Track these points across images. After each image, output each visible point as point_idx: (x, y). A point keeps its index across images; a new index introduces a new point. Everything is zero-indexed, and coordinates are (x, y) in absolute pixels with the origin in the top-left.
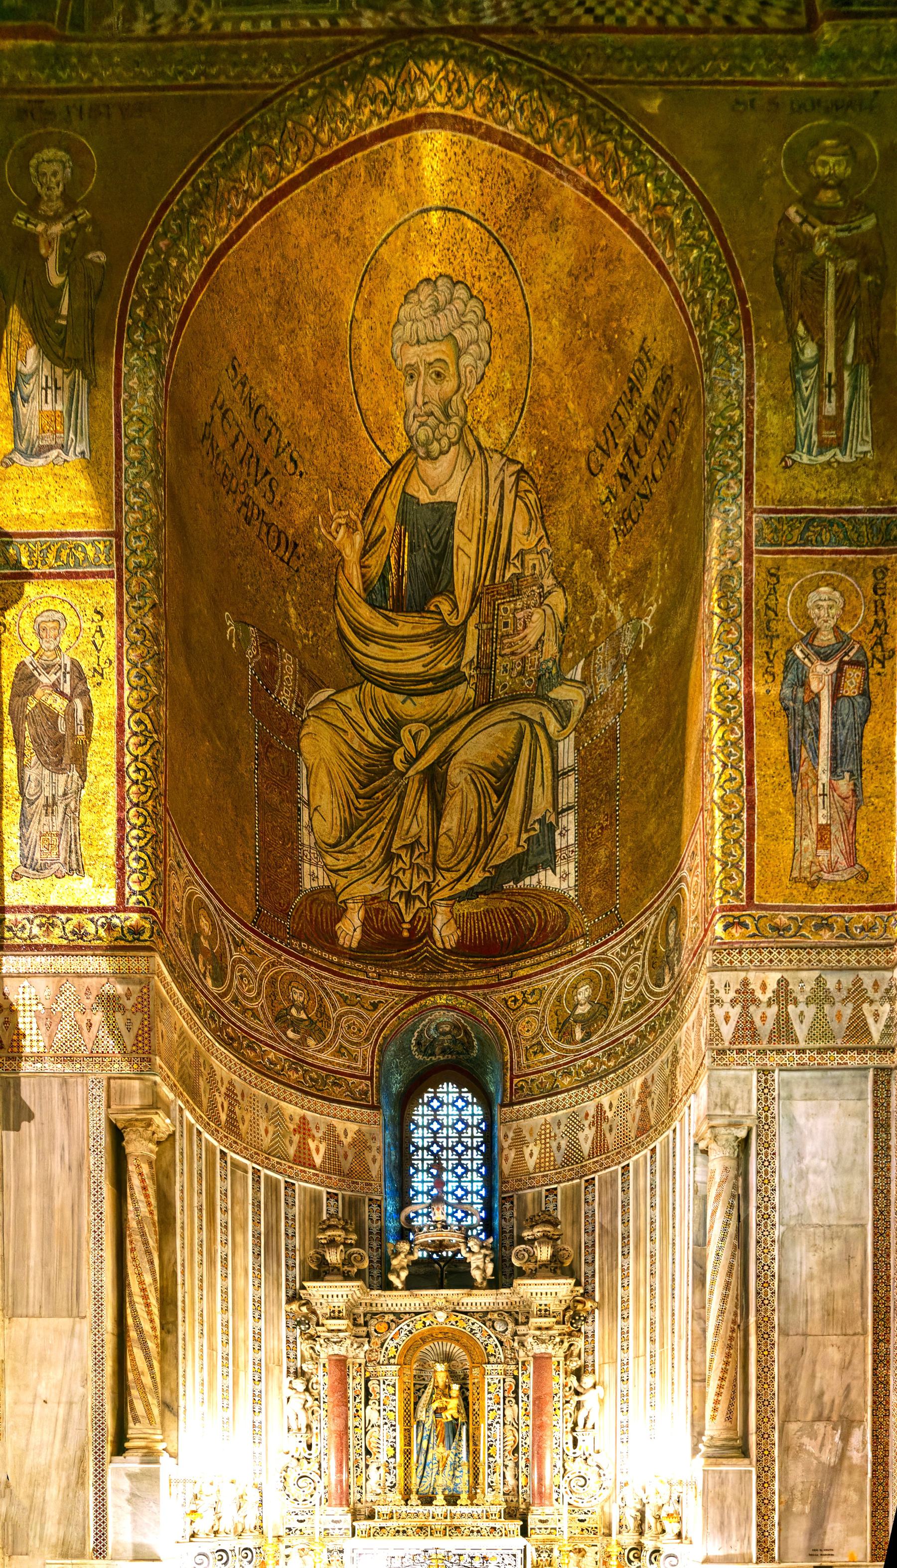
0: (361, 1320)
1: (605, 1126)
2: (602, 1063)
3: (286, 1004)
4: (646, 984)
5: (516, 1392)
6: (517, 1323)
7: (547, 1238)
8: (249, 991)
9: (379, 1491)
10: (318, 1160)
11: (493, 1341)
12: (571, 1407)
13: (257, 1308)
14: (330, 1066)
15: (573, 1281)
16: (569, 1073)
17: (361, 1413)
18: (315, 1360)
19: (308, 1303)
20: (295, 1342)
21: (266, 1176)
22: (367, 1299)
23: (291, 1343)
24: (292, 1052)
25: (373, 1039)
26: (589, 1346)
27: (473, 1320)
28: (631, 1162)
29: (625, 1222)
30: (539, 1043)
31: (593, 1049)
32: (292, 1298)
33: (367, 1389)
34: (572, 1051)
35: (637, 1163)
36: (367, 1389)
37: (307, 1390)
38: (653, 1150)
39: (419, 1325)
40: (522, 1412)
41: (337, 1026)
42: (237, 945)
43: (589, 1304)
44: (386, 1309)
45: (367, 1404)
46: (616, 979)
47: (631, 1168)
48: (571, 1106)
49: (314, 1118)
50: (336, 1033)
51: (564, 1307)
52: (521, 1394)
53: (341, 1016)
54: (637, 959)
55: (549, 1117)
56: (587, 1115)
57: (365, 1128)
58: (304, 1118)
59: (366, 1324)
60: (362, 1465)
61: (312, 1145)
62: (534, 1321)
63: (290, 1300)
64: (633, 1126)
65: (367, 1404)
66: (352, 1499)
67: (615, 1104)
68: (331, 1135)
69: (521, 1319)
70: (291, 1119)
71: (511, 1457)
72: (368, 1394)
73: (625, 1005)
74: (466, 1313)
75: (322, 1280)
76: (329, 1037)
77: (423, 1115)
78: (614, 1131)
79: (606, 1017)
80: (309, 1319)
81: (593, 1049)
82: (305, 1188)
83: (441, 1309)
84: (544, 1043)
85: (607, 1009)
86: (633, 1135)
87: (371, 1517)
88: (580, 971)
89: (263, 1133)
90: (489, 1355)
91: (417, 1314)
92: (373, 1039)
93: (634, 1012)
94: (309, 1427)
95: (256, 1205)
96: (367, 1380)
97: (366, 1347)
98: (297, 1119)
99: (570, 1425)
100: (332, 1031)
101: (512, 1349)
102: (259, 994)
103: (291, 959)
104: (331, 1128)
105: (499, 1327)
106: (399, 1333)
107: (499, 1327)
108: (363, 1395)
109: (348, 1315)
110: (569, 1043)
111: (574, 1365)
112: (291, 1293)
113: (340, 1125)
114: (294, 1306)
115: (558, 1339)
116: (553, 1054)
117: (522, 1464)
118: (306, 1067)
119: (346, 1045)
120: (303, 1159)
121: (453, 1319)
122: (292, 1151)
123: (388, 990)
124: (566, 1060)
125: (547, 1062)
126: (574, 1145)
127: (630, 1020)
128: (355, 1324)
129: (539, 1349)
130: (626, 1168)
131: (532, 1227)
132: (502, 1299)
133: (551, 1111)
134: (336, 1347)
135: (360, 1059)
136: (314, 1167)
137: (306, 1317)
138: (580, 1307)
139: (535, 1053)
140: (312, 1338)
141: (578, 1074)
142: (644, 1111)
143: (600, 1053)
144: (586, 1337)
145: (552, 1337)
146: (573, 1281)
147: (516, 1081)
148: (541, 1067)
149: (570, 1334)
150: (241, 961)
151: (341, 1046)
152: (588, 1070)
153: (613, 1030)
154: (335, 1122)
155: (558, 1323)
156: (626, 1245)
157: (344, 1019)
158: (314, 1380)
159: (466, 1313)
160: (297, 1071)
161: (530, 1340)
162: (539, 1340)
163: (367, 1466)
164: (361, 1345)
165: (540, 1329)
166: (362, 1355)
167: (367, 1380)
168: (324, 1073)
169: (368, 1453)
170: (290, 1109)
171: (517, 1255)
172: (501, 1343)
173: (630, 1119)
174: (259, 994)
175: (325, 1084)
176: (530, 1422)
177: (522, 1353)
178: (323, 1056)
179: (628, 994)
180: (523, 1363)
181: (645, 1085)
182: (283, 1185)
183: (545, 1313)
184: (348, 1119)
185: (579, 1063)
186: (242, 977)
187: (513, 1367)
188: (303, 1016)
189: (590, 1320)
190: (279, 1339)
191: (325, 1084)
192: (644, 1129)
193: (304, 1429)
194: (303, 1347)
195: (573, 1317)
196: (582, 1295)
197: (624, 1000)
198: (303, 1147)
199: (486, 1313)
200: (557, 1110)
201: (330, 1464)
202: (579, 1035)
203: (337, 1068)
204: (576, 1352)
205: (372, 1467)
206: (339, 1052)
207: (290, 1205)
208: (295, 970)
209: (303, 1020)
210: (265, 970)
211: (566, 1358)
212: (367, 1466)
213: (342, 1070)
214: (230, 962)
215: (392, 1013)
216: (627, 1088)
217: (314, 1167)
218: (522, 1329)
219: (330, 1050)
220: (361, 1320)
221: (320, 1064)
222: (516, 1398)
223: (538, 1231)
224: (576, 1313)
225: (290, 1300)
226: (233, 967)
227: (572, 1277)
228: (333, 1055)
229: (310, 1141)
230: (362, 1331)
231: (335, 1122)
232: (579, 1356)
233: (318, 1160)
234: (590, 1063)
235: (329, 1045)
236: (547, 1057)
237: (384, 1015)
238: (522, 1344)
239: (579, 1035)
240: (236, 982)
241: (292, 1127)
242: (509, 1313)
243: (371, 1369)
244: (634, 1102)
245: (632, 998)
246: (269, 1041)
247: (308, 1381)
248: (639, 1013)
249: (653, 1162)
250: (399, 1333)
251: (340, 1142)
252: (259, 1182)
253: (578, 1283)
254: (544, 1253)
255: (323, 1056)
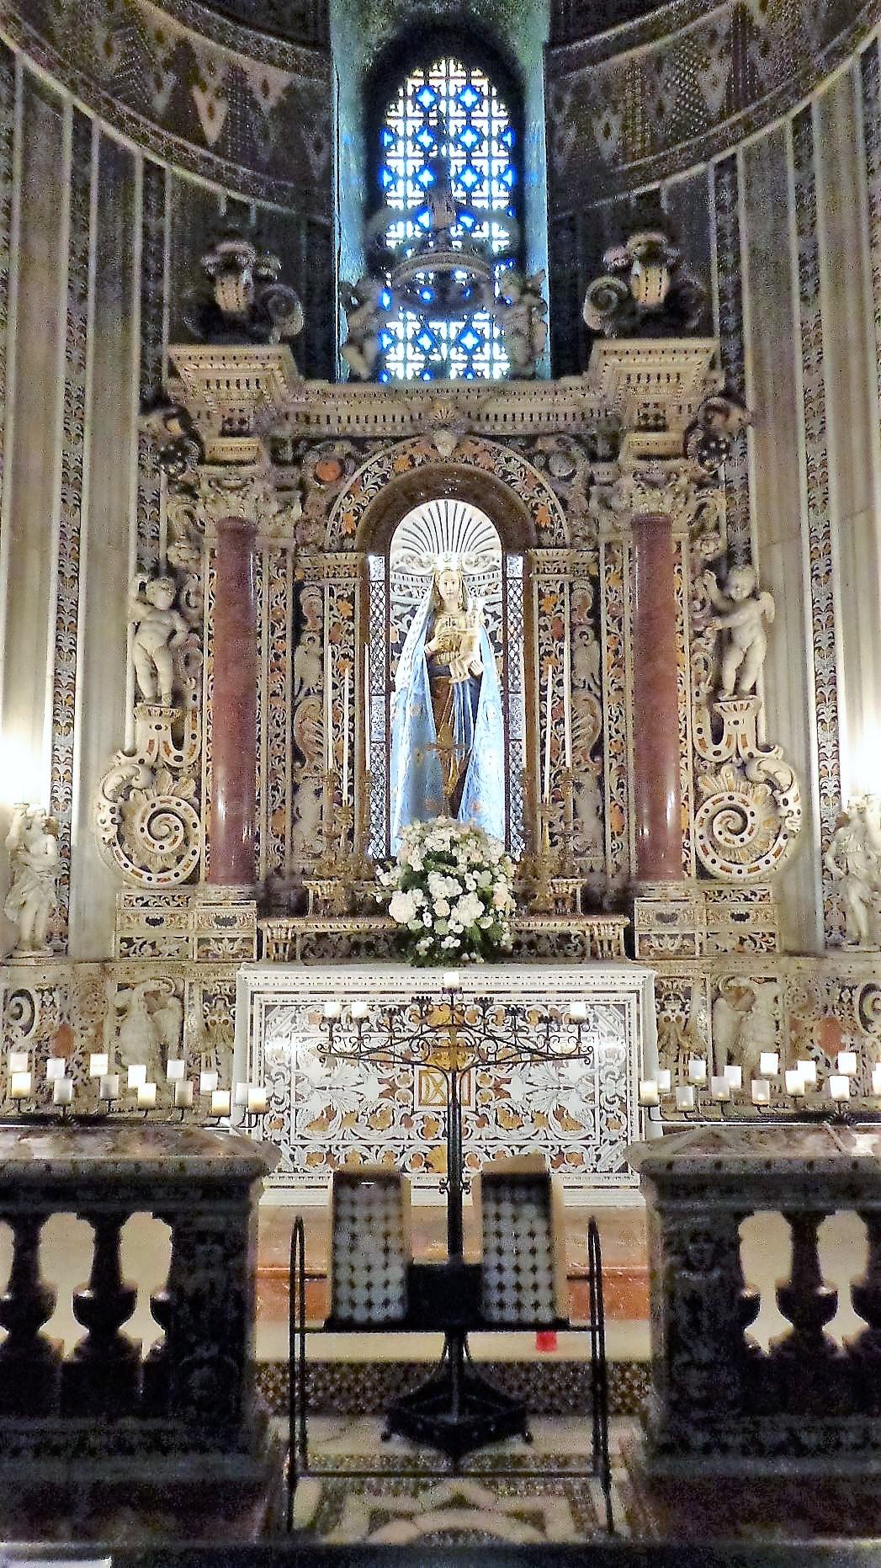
0: (288, 454)
5: (595, 613)
7: (652, 256)
9: (319, 847)
10: (212, 130)
11: (548, 498)
12: (708, 645)
13: (74, 413)
17: (286, 662)
18: (195, 539)
19: (184, 416)
20: (156, 503)
21: (108, 143)
22: (298, 403)
23: (148, 504)
26: (737, 510)
27: (509, 453)
28: (814, 99)
29: (807, 229)
32: (155, 401)
33: (297, 606)
36: (297, 606)
37: (175, 606)
39: (402, 464)
40: (608, 657)
43: (736, 413)
44: (335, 429)
45: (296, 642)
47: (815, 114)
49: (205, 47)
52: (605, 618)
57: (301, 81)
59: (297, 461)
60: (285, 783)
61: (201, 99)
63: (147, 407)
65: (296, 642)
66: (262, 870)
68: (236, 86)
69: (602, 448)
71: (590, 764)
72: (299, 619)
74: (494, 438)
77: (405, 117)
80: (186, 451)
82: (183, 183)
83: (445, 426)
87: (299, 910)
90: (539, 529)
91: (397, 440)
94: (177, 697)
95: (81, 189)
96: (298, 587)
97: (297, 512)
98: (171, 42)
99: (705, 688)
101: (585, 515)
106: (361, 482)
107: (560, 469)
108: (288, 622)
111: (711, 548)
112: (150, 391)
114: (155, 419)
117: (611, 780)
120: (183, 120)
121: (469, 449)
122: (161, 102)
126: (696, 98)
128: (277, 461)
129: (647, 503)
130: (804, 118)
131: (623, 241)
132: (565, 405)
134: (233, 498)
136: (202, 141)
137: (179, 444)
140: (189, 490)
144: (730, 490)
149: (701, 485)
158: (191, 585)
159: (494, 438)
163: (295, 788)
164: (287, 505)
166: (288, 530)
167: (298, 587)
169: (297, 755)
171: (595, 299)
176: (629, 681)
177: (605, 525)
180: (608, 546)
182: (139, 168)
184: (271, 62)
187: (588, 556)
189: (737, 448)
190: (123, 490)
193: (166, 701)
194: (172, 508)
195: (704, 444)
199: (531, 439)
201: (216, 782)
204: (710, 525)
205: (307, 789)
211: (693, 537)
212: (295, 788)
217: (202, 141)
218: (602, 471)
220: (288, 454)
222: (596, 628)
223: (637, 242)
224: (710, 436)
225: (147, 407)
230: (291, 474)
232: (717, 528)
233: (212, 130)
238: (605, 504)
241: (161, 54)
242: (578, 439)
243: (305, 562)
247: (179, 590)
250: (361, 482)
254: (651, 288)
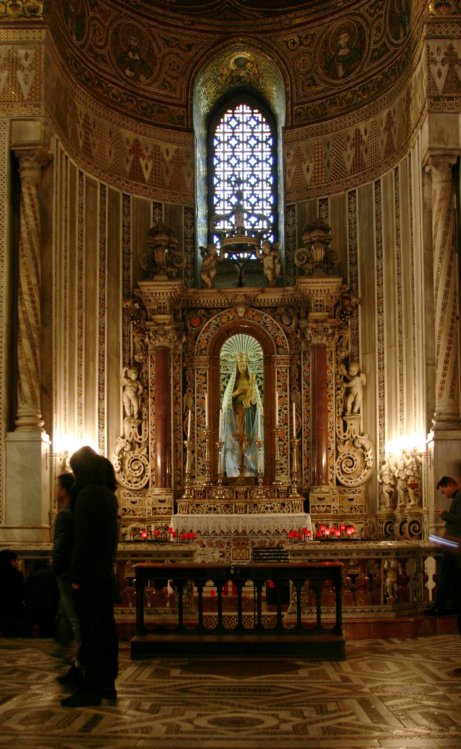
1: (362, 148)
2: (359, 96)
3: (125, 49)
4: (387, 37)
6: (299, 317)
8: (100, 41)
14: (156, 97)
15: (340, 280)
16: (335, 103)
24: (128, 87)
25: (188, 74)
28: (381, 178)
30: (312, 78)
31: (351, 84)
34: (336, 85)
35: (385, 178)
38: (396, 170)
41: (161, 64)
42: (92, 6)
46: (367, 30)
48: (337, 130)
50: (160, 69)
51: (334, 302)
53: (164, 56)
54: (381, 16)
55: (321, 139)
56: (349, 138)
58: (136, 141)
62: (314, 315)
64: (382, 149)
67: (369, 129)
70: (128, 142)
73: (374, 51)
75: (152, 280)
76: (156, 73)
78: (369, 152)
79: (361, 60)
81: (351, 84)
84: (316, 78)
85: (361, 53)
86: (382, 156)
88: (340, 23)
89: (107, 154)
92: (188, 74)
93: (380, 57)
100: (157, 68)
102: (106, 42)
103: (129, 13)
104: (157, 148)
105: (286, 321)
109: (170, 311)
110: (334, 78)
113: (163, 146)
115: (330, 331)
116: (322, 87)
118: (139, 98)
119: (168, 79)
123: (199, 34)
124: (332, 92)
125: (319, 93)
127: (377, 63)
133: (322, 134)
135: (178, 90)
138: (347, 302)
139: (309, 86)
141: (341, 104)
142: (390, 136)
143: (357, 88)
145: (325, 329)
146: (340, 280)
147: (295, 108)
148: (314, 97)
150: (94, 18)
151: (164, 80)
152: (349, 101)
153: (365, 70)
154: (160, 143)
155: (330, 317)
156: (379, 249)
157: (167, 59)
160: (132, 101)
161: (309, 331)
162: (316, 332)
165: (316, 321)
168: (152, 103)
170: (128, 134)
172: (287, 335)
173: (379, 143)
174: (106, 42)
175: (153, 112)
178: (152, 89)
179: (375, 43)
181: (389, 114)
183: (320, 307)
185: (341, 95)
186: (95, 30)
188: (137, 57)
191: (153, 112)
192: (390, 151)
196: (348, 292)
197: (373, 47)
198: (136, 165)
200: (327, 133)
202: (341, 73)
203: (161, 98)
206: (163, 85)
207: (127, 215)
208: (132, 22)
209: (137, 61)
210: (111, 23)
213: (165, 99)
214: (87, 19)
215: (201, 52)
216: (377, 117)
219: (156, 84)
221: (149, 95)
226: (89, 23)
227: (340, 277)
228: (158, 87)
229: (141, 159)
231: (160, 143)
234: (350, 95)
235: (156, 80)
236: (318, 89)
237: (196, 54)
239: (341, 73)
240: (91, 35)
244: (382, 129)
245: (378, 46)
246: (113, 79)
248: (384, 58)
249: (397, 180)
251: (163, 160)
252: (104, 196)
253: (344, 282)
255: (152, 89)
